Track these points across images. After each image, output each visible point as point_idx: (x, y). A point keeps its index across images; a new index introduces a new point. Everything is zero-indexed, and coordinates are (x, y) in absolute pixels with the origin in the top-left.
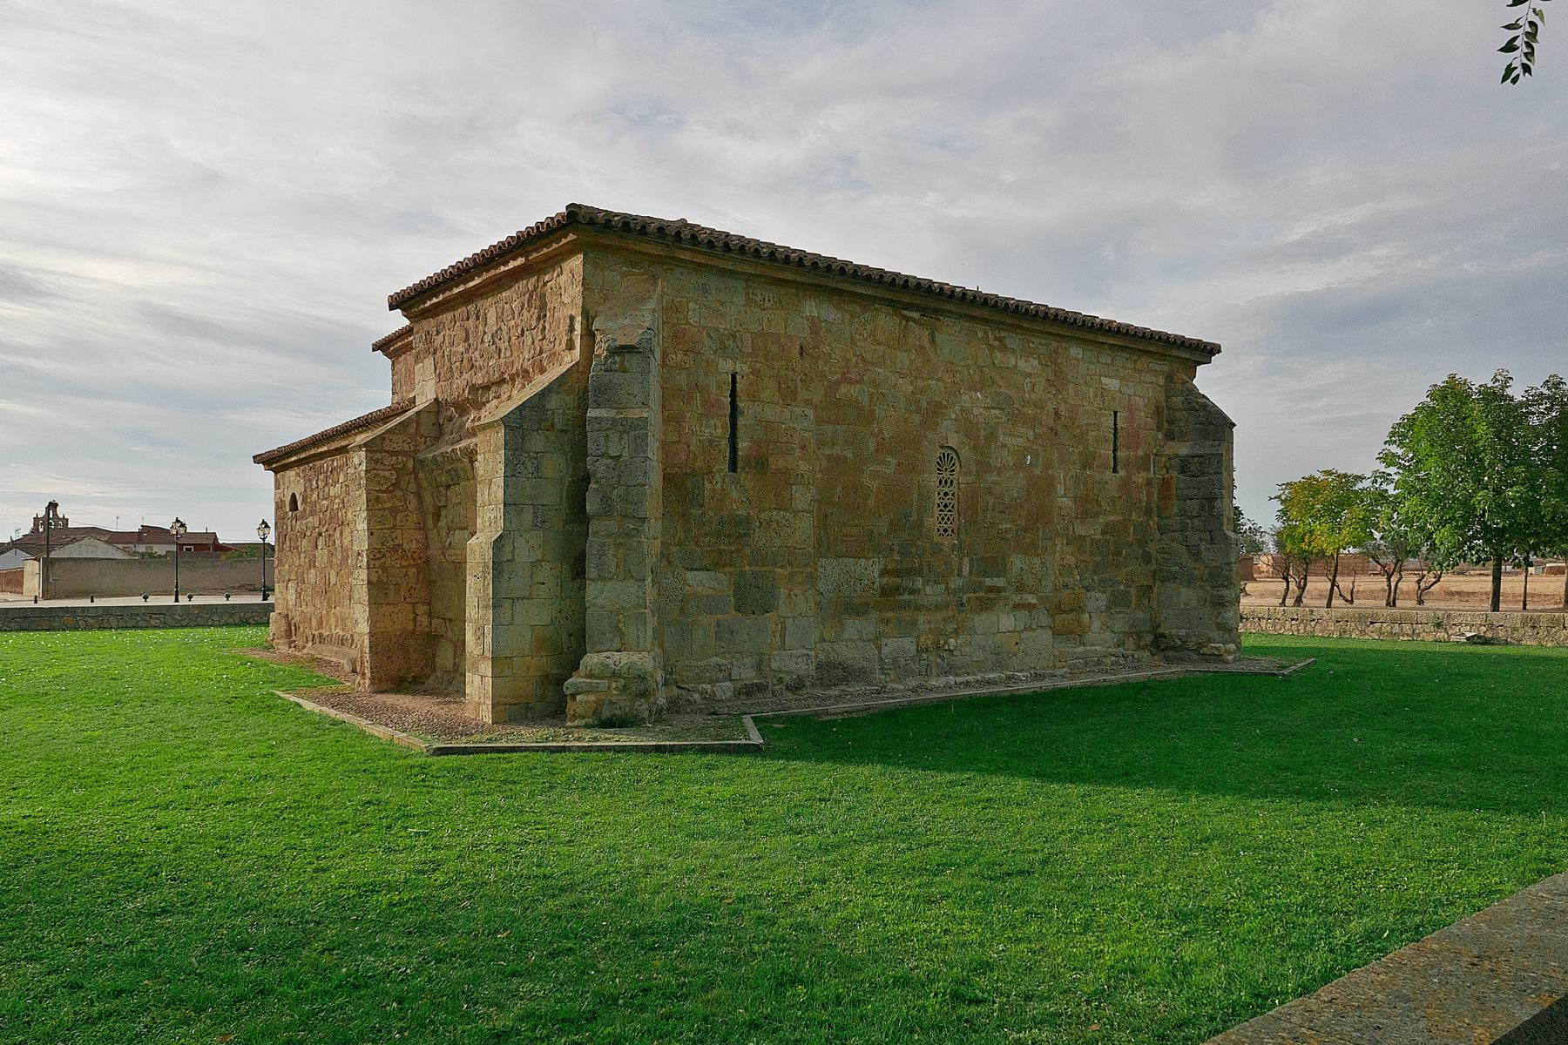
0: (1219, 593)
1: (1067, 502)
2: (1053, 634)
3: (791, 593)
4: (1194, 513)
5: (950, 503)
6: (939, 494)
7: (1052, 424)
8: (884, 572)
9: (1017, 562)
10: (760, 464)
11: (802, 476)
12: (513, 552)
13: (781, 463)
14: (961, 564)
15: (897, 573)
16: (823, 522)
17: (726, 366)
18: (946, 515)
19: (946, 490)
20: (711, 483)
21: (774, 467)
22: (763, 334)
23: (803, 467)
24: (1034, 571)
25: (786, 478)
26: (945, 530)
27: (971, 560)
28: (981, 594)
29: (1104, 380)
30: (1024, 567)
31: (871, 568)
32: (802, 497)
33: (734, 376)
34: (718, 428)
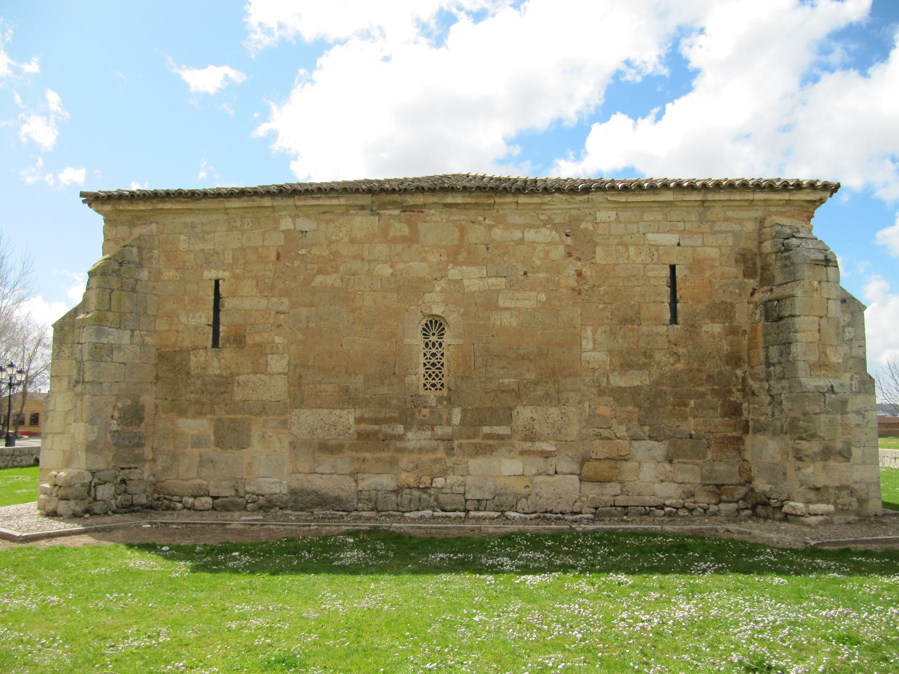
0: (798, 446)
1: (601, 356)
2: (580, 480)
3: (265, 435)
4: (775, 360)
5: (439, 363)
6: (425, 355)
7: (573, 284)
8: (359, 421)
9: (524, 414)
10: (239, 340)
11: (277, 347)
12: (55, 405)
13: (258, 339)
14: (450, 415)
15: (376, 421)
16: (296, 383)
17: (213, 274)
18: (434, 373)
19: (434, 350)
20: (195, 356)
21: (251, 342)
22: (243, 249)
23: (278, 340)
24: (549, 421)
25: (261, 350)
26: (433, 385)
27: (464, 412)
28: (476, 440)
29: (650, 236)
30: (535, 416)
31: (348, 418)
32: (278, 363)
33: (217, 282)
34: (205, 317)
